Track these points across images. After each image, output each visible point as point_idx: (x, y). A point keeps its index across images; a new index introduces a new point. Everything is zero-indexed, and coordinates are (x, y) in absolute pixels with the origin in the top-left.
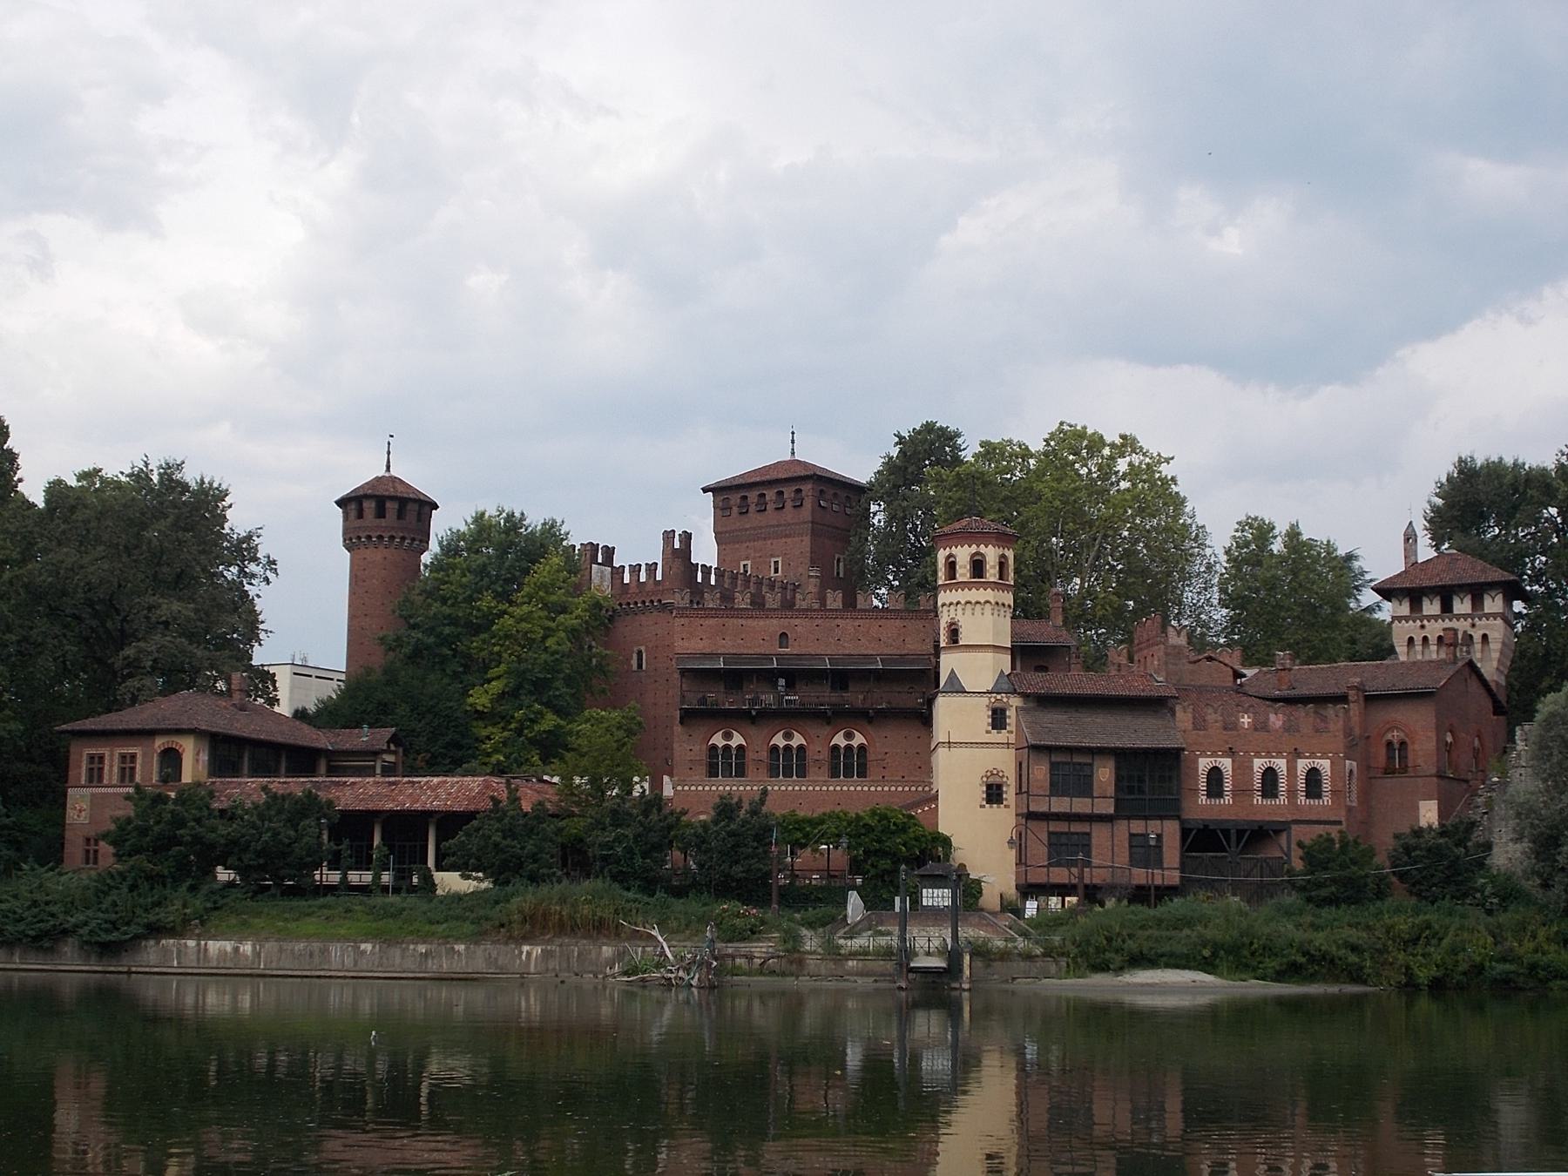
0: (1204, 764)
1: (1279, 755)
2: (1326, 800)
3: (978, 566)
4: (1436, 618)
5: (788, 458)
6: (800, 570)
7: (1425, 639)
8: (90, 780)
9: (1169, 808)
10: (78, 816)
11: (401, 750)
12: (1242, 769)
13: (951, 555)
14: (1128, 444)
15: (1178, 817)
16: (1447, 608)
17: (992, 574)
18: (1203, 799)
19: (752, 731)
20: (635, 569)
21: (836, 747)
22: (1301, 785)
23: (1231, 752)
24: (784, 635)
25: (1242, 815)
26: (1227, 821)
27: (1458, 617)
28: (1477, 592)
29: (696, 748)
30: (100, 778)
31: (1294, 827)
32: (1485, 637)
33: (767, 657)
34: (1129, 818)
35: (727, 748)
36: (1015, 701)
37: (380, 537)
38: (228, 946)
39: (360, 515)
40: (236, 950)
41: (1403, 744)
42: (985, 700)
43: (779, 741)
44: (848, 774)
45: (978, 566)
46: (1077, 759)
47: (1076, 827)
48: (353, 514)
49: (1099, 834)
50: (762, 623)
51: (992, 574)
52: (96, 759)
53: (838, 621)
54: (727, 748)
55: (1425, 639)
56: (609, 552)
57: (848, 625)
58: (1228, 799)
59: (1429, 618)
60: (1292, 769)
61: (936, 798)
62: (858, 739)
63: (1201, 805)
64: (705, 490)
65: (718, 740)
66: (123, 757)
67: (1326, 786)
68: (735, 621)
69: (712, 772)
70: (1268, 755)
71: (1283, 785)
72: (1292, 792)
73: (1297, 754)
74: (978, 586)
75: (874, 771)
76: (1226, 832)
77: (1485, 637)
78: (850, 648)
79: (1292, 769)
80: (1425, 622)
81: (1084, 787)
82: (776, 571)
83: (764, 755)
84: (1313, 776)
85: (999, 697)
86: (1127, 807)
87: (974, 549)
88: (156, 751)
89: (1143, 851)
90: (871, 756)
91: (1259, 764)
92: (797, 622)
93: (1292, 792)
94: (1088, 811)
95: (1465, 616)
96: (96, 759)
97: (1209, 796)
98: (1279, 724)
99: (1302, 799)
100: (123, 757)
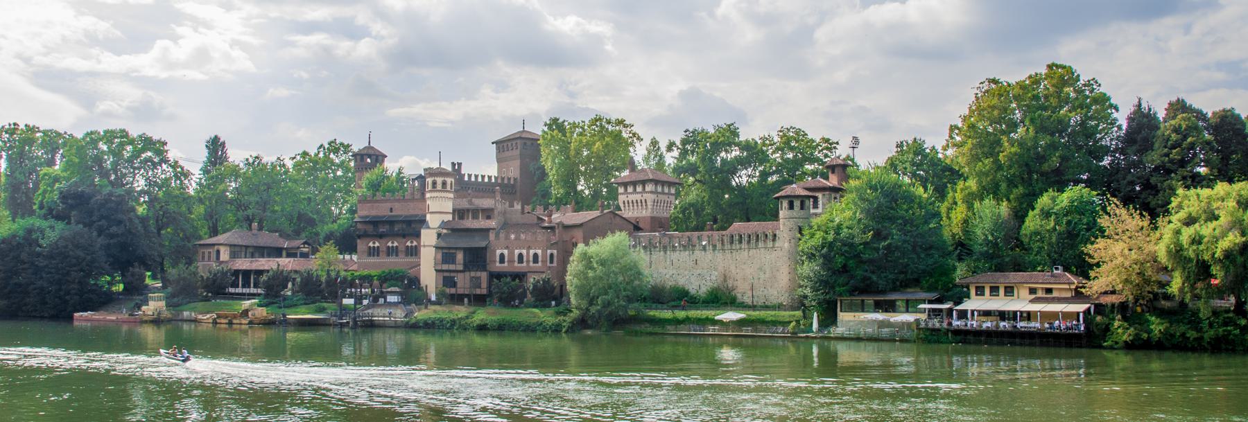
0: (498, 252)
1: (524, 248)
2: (540, 264)
3: (434, 183)
4: (631, 193)
7: (628, 201)
9: (483, 267)
11: (310, 247)
12: (511, 254)
15: (486, 271)
17: (439, 187)
18: (498, 264)
19: (381, 241)
21: (408, 246)
22: (531, 259)
23: (507, 248)
24: (391, 209)
25: (511, 270)
26: (506, 272)
27: (638, 193)
31: (528, 274)
32: (646, 200)
33: (385, 216)
34: (470, 271)
37: (362, 169)
42: (435, 231)
43: (390, 244)
44: (412, 255)
45: (434, 183)
46: (451, 251)
47: (452, 274)
48: (358, 160)
49: (460, 276)
51: (439, 187)
55: (628, 201)
57: (411, 205)
58: (506, 264)
60: (528, 253)
61: (420, 265)
62: (415, 243)
63: (498, 266)
64: (493, 143)
65: (371, 244)
67: (540, 259)
69: (369, 255)
70: (520, 249)
71: (525, 259)
72: (528, 261)
73: (529, 248)
74: (434, 191)
78: (412, 212)
79: (528, 253)
81: (454, 262)
84: (536, 256)
86: (467, 267)
87: (433, 178)
89: (476, 283)
91: (517, 252)
93: (528, 261)
94: (454, 269)
95: (640, 193)
97: (519, 263)
98: (524, 237)
99: (531, 264)
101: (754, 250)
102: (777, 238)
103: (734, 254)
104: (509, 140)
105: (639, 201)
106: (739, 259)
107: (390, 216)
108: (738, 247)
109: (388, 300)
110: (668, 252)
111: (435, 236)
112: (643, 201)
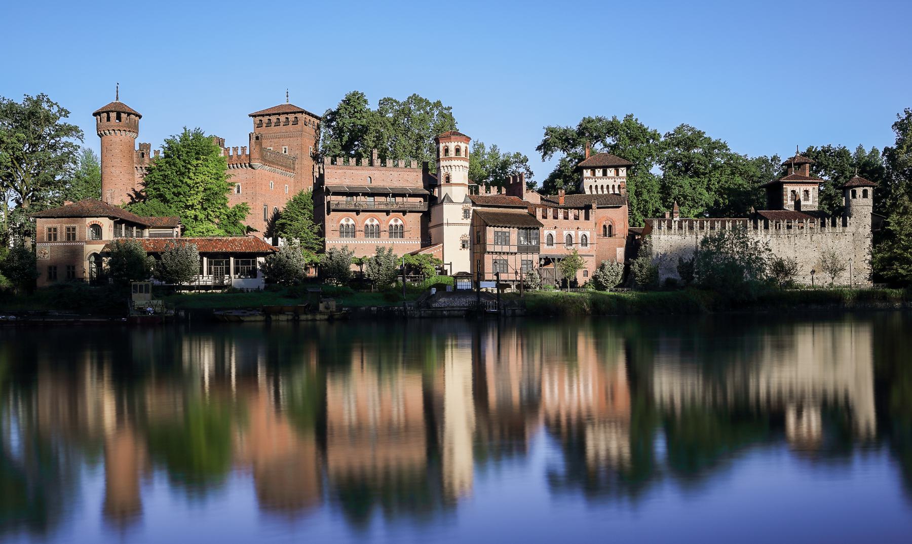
3: (458, 151)
4: (600, 178)
6: (297, 152)
7: (596, 186)
8: (50, 239)
10: (43, 256)
12: (560, 235)
14: (438, 104)
16: (605, 174)
18: (546, 245)
20: (235, 149)
27: (609, 178)
28: (617, 168)
29: (335, 225)
30: (55, 238)
39: (108, 119)
41: (610, 226)
42: (461, 206)
45: (458, 151)
49: (511, 259)
50: (360, 172)
52: (52, 230)
53: (391, 172)
54: (396, 226)
55: (596, 186)
56: (223, 140)
58: (555, 246)
59: (598, 178)
60: (577, 235)
64: (250, 116)
66: (68, 229)
68: (349, 171)
74: (458, 159)
75: (406, 234)
76: (553, 259)
79: (577, 235)
80: (596, 179)
81: (507, 242)
82: (285, 152)
85: (467, 205)
87: (456, 143)
88: (87, 226)
90: (405, 229)
91: (565, 233)
92: (375, 172)
95: (612, 178)
96: (52, 230)
100: (68, 229)
101: (819, 235)
102: (848, 224)
103: (792, 239)
105: (611, 187)
106: (798, 244)
108: (798, 231)
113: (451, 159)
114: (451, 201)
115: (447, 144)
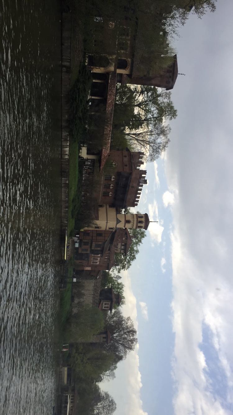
5: (178, 73)
12: (99, 257)
13: (143, 222)
32: (117, 250)
35: (111, 178)
36: (114, 231)
38: (67, 153)
40: (66, 154)
42: (115, 227)
47: (89, 244)
77: (117, 250)
83: (109, 183)
93: (94, 261)
99: (92, 262)
104: (174, 70)
107: (129, 186)
109: (76, 244)
110: (93, 296)
111: (111, 209)
112: (117, 249)
113: (137, 219)
114: (117, 224)
115: (144, 223)
